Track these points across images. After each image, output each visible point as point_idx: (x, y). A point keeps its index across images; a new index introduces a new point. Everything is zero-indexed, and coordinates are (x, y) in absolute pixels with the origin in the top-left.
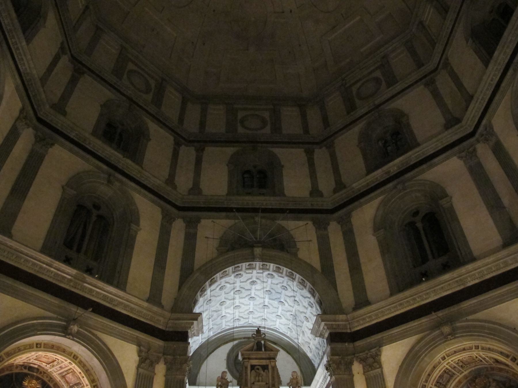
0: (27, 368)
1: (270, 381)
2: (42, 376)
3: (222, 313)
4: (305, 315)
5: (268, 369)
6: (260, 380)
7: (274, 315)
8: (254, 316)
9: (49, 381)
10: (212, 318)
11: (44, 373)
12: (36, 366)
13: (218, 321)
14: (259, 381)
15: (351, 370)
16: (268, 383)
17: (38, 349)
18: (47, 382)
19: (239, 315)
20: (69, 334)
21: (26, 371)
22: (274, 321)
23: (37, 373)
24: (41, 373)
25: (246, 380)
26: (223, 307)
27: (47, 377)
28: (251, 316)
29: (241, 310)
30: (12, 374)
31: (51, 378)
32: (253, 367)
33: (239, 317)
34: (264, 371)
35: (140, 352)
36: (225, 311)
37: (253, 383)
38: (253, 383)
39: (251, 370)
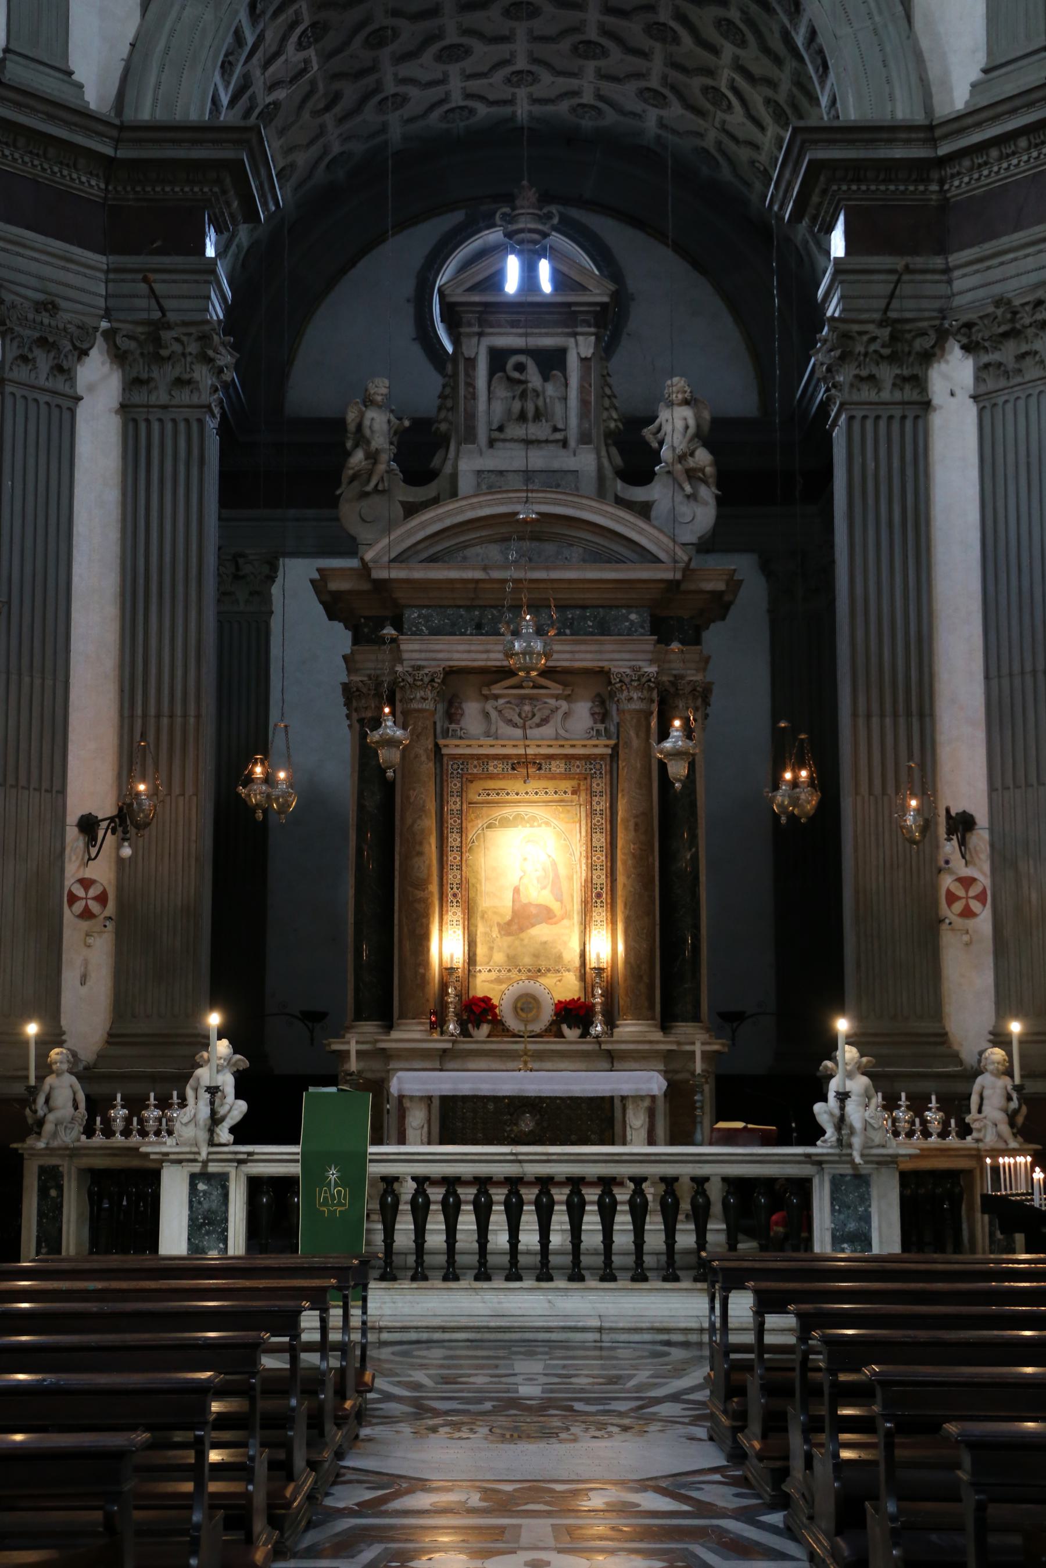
1: (573, 421)
3: (379, 83)
4: (769, 92)
5: (562, 365)
6: (531, 414)
7: (631, 87)
8: (538, 91)
10: (338, 109)
13: (369, 114)
14: (522, 417)
15: (919, 382)
16: (560, 426)
19: (464, 88)
22: (634, 114)
25: (471, 417)
26: (385, 54)
28: (522, 93)
29: (469, 64)
32: (498, 358)
33: (468, 96)
34: (546, 378)
36: (395, 75)
37: (501, 429)
38: (501, 429)
39: (491, 375)
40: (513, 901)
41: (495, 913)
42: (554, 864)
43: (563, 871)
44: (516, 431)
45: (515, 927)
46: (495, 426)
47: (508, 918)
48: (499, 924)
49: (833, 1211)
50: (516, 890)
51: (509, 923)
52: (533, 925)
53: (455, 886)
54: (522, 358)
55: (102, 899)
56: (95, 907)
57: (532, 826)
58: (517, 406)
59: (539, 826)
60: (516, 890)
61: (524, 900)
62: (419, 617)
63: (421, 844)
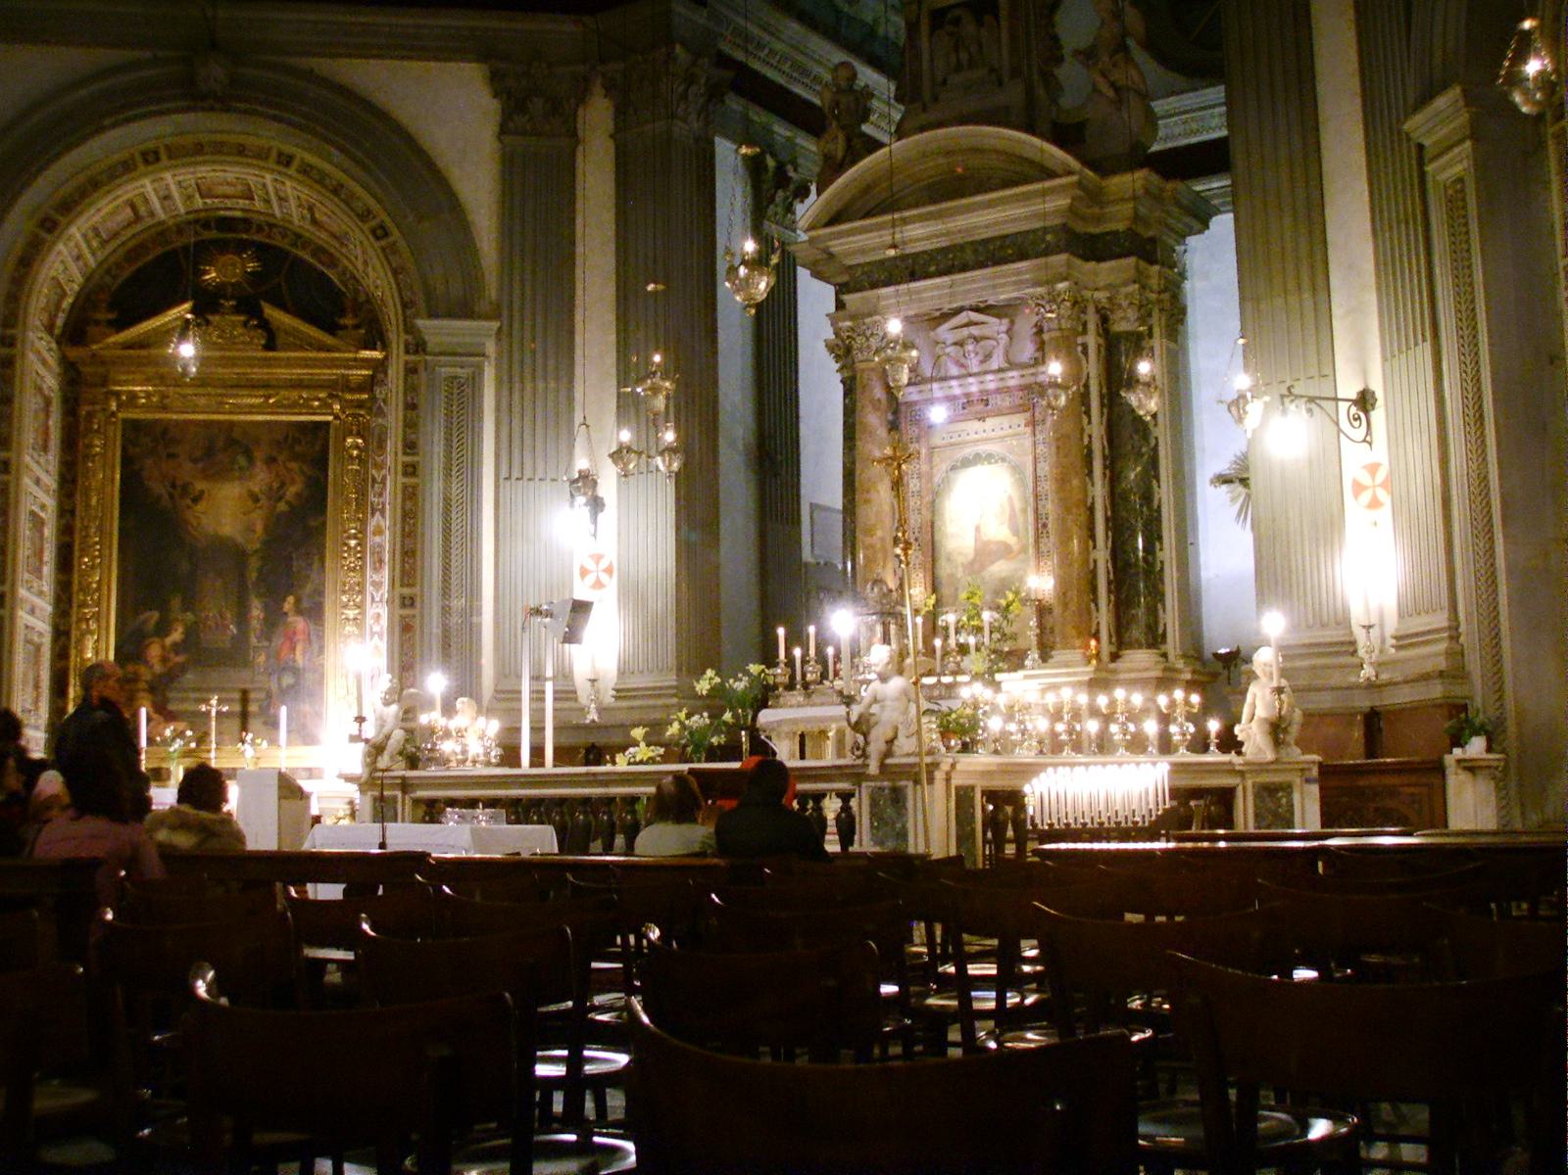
0: (213, 224)
2: (269, 236)
9: (294, 245)
11: (271, 226)
12: (238, 214)
17: (150, 168)
18: (288, 248)
20: (203, 98)
21: (214, 234)
23: (247, 231)
24: (260, 229)
27: (284, 237)
30: (174, 251)
31: (298, 236)
34: (980, 23)
35: (495, 79)
37: (944, 82)
38: (944, 82)
40: (976, 541)
41: (960, 554)
42: (1010, 498)
43: (1018, 505)
44: (956, 79)
45: (977, 566)
46: (940, 79)
47: (971, 556)
48: (963, 564)
49: (872, 827)
50: (978, 529)
51: (972, 563)
52: (993, 563)
53: (916, 530)
54: (957, 12)
55: (609, 571)
56: (604, 578)
57: (990, 463)
58: (953, 59)
59: (996, 462)
60: (978, 529)
61: (985, 538)
62: (863, 273)
63: (868, 492)
